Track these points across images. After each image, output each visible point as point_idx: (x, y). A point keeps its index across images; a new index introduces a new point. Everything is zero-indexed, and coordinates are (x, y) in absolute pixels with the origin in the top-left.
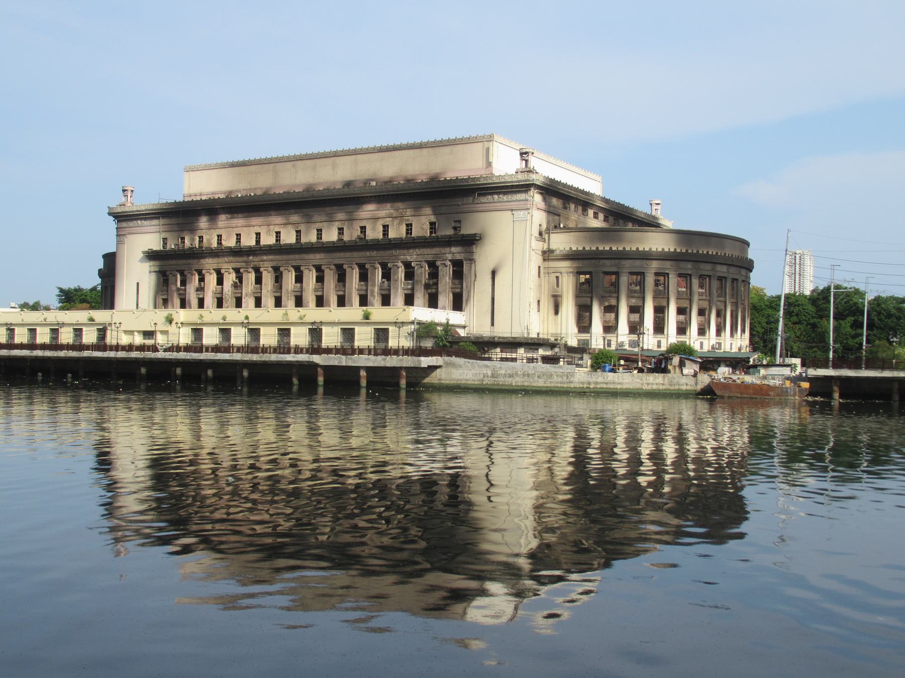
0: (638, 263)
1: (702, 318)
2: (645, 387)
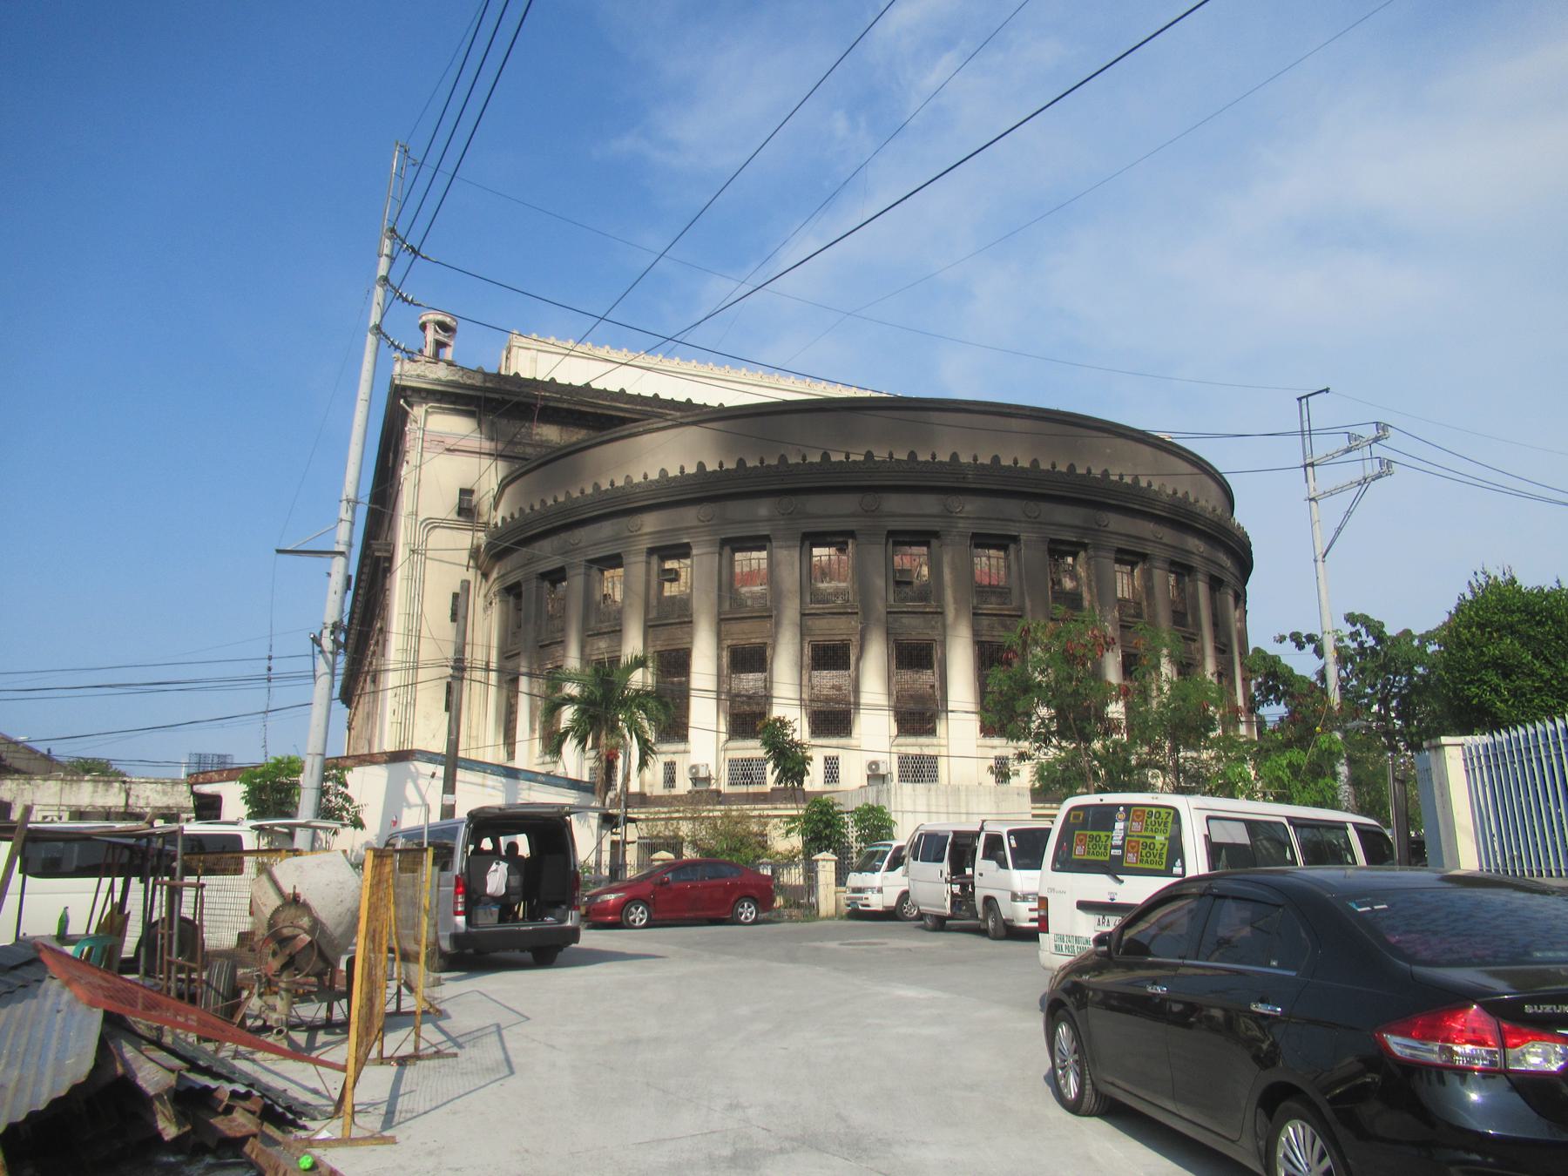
0: (606, 529)
1: (827, 680)
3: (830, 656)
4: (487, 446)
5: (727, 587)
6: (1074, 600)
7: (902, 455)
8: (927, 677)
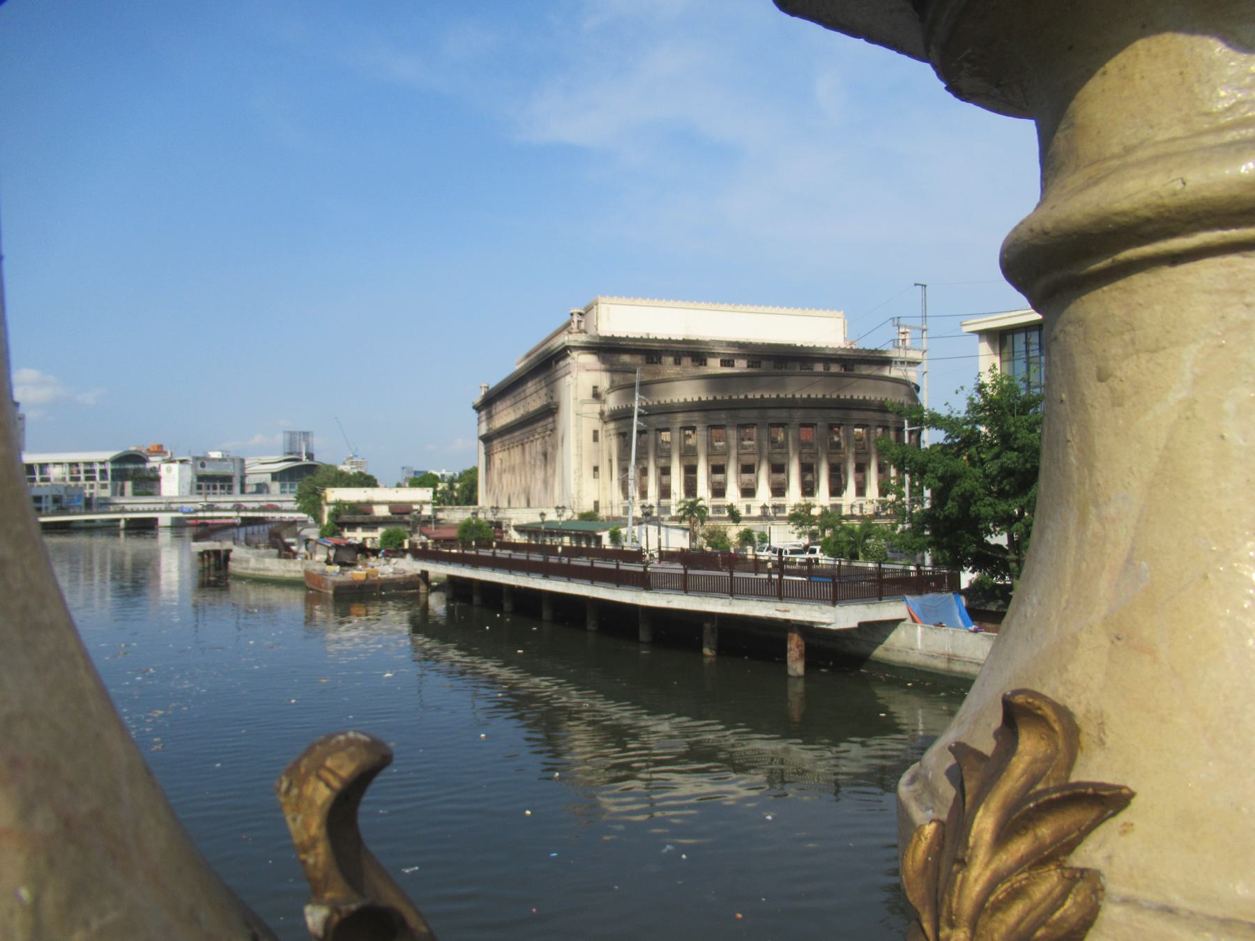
0: (663, 418)
1: (746, 477)
2: (288, 575)
3: (748, 469)
4: (603, 366)
5: (710, 445)
6: (838, 445)
7: (774, 396)
8: (782, 476)
